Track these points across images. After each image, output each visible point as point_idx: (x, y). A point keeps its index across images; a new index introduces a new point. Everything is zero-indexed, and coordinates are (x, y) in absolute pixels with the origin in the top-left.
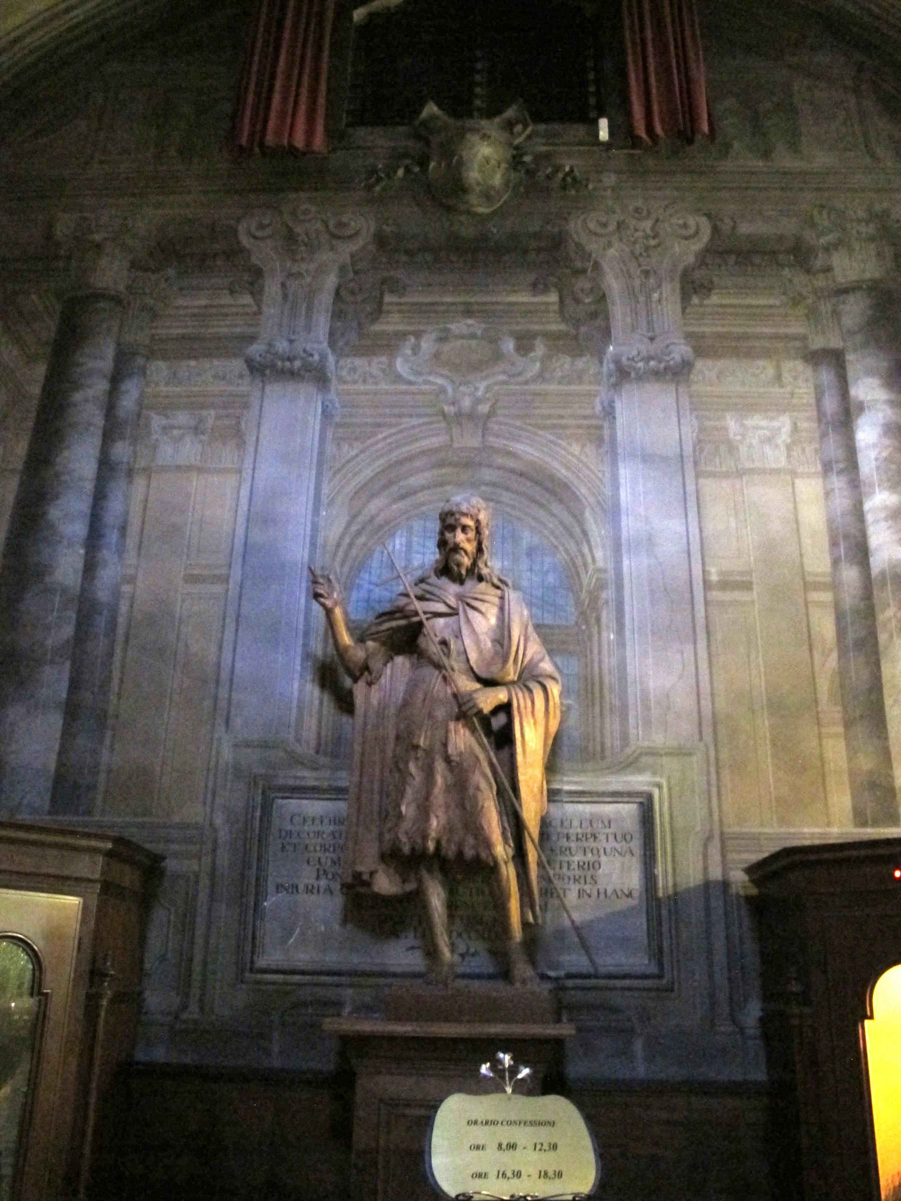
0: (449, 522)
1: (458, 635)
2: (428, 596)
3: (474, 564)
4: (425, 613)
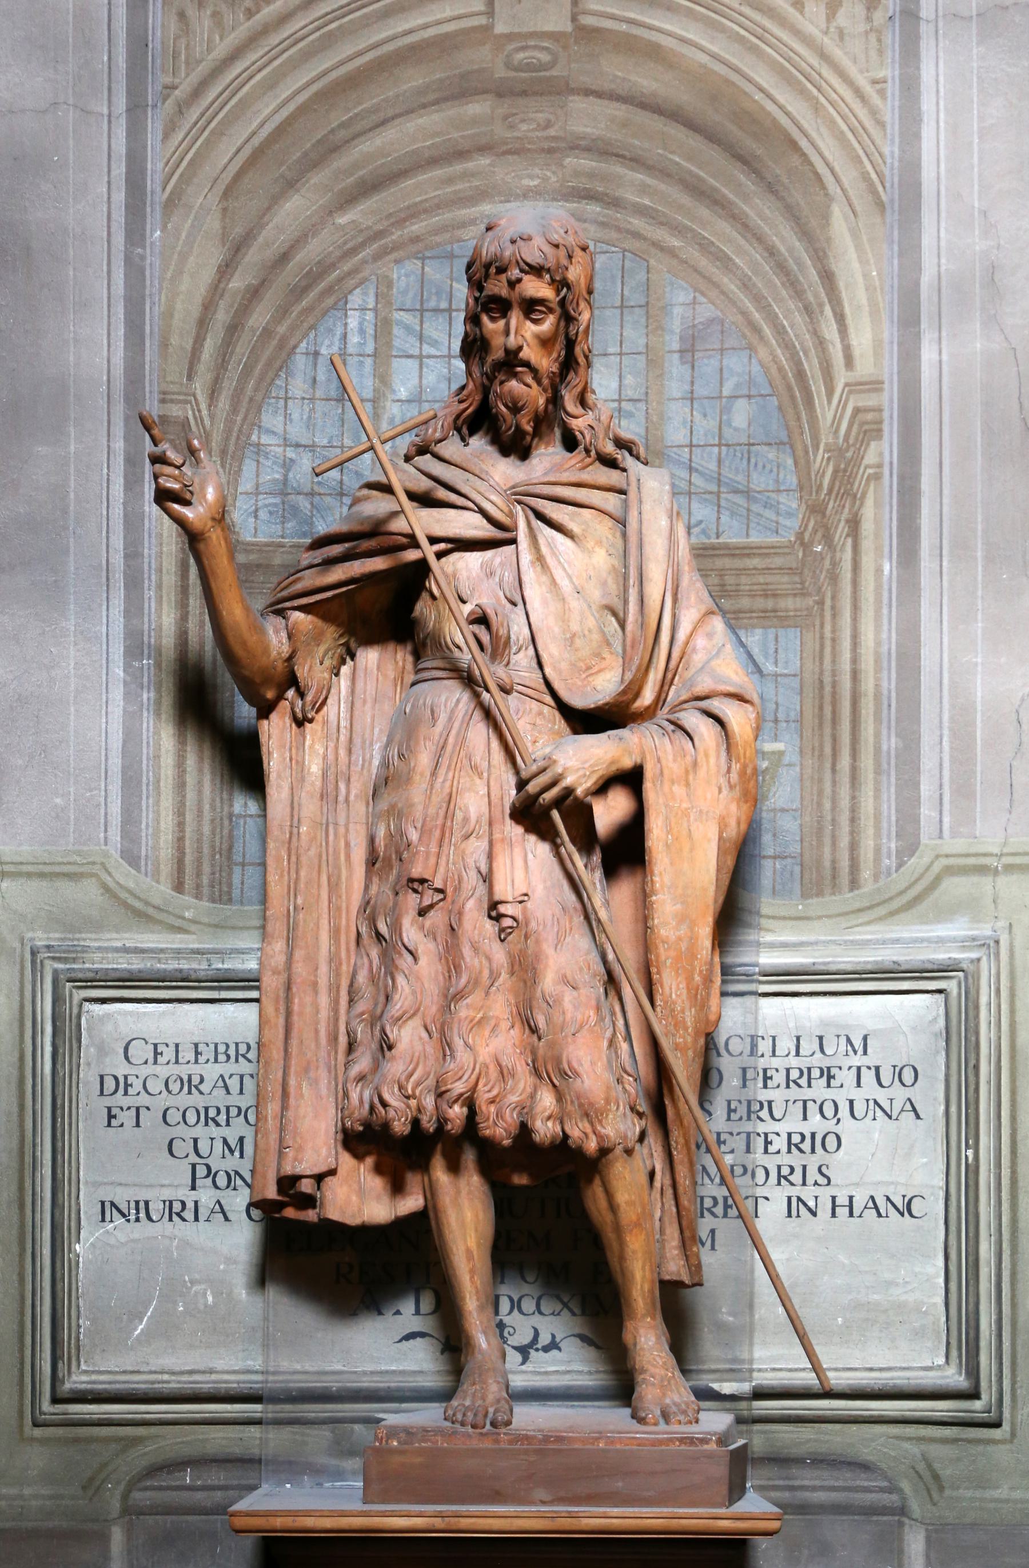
0: (490, 290)
1: (518, 600)
2: (442, 494)
3: (555, 400)
4: (433, 540)
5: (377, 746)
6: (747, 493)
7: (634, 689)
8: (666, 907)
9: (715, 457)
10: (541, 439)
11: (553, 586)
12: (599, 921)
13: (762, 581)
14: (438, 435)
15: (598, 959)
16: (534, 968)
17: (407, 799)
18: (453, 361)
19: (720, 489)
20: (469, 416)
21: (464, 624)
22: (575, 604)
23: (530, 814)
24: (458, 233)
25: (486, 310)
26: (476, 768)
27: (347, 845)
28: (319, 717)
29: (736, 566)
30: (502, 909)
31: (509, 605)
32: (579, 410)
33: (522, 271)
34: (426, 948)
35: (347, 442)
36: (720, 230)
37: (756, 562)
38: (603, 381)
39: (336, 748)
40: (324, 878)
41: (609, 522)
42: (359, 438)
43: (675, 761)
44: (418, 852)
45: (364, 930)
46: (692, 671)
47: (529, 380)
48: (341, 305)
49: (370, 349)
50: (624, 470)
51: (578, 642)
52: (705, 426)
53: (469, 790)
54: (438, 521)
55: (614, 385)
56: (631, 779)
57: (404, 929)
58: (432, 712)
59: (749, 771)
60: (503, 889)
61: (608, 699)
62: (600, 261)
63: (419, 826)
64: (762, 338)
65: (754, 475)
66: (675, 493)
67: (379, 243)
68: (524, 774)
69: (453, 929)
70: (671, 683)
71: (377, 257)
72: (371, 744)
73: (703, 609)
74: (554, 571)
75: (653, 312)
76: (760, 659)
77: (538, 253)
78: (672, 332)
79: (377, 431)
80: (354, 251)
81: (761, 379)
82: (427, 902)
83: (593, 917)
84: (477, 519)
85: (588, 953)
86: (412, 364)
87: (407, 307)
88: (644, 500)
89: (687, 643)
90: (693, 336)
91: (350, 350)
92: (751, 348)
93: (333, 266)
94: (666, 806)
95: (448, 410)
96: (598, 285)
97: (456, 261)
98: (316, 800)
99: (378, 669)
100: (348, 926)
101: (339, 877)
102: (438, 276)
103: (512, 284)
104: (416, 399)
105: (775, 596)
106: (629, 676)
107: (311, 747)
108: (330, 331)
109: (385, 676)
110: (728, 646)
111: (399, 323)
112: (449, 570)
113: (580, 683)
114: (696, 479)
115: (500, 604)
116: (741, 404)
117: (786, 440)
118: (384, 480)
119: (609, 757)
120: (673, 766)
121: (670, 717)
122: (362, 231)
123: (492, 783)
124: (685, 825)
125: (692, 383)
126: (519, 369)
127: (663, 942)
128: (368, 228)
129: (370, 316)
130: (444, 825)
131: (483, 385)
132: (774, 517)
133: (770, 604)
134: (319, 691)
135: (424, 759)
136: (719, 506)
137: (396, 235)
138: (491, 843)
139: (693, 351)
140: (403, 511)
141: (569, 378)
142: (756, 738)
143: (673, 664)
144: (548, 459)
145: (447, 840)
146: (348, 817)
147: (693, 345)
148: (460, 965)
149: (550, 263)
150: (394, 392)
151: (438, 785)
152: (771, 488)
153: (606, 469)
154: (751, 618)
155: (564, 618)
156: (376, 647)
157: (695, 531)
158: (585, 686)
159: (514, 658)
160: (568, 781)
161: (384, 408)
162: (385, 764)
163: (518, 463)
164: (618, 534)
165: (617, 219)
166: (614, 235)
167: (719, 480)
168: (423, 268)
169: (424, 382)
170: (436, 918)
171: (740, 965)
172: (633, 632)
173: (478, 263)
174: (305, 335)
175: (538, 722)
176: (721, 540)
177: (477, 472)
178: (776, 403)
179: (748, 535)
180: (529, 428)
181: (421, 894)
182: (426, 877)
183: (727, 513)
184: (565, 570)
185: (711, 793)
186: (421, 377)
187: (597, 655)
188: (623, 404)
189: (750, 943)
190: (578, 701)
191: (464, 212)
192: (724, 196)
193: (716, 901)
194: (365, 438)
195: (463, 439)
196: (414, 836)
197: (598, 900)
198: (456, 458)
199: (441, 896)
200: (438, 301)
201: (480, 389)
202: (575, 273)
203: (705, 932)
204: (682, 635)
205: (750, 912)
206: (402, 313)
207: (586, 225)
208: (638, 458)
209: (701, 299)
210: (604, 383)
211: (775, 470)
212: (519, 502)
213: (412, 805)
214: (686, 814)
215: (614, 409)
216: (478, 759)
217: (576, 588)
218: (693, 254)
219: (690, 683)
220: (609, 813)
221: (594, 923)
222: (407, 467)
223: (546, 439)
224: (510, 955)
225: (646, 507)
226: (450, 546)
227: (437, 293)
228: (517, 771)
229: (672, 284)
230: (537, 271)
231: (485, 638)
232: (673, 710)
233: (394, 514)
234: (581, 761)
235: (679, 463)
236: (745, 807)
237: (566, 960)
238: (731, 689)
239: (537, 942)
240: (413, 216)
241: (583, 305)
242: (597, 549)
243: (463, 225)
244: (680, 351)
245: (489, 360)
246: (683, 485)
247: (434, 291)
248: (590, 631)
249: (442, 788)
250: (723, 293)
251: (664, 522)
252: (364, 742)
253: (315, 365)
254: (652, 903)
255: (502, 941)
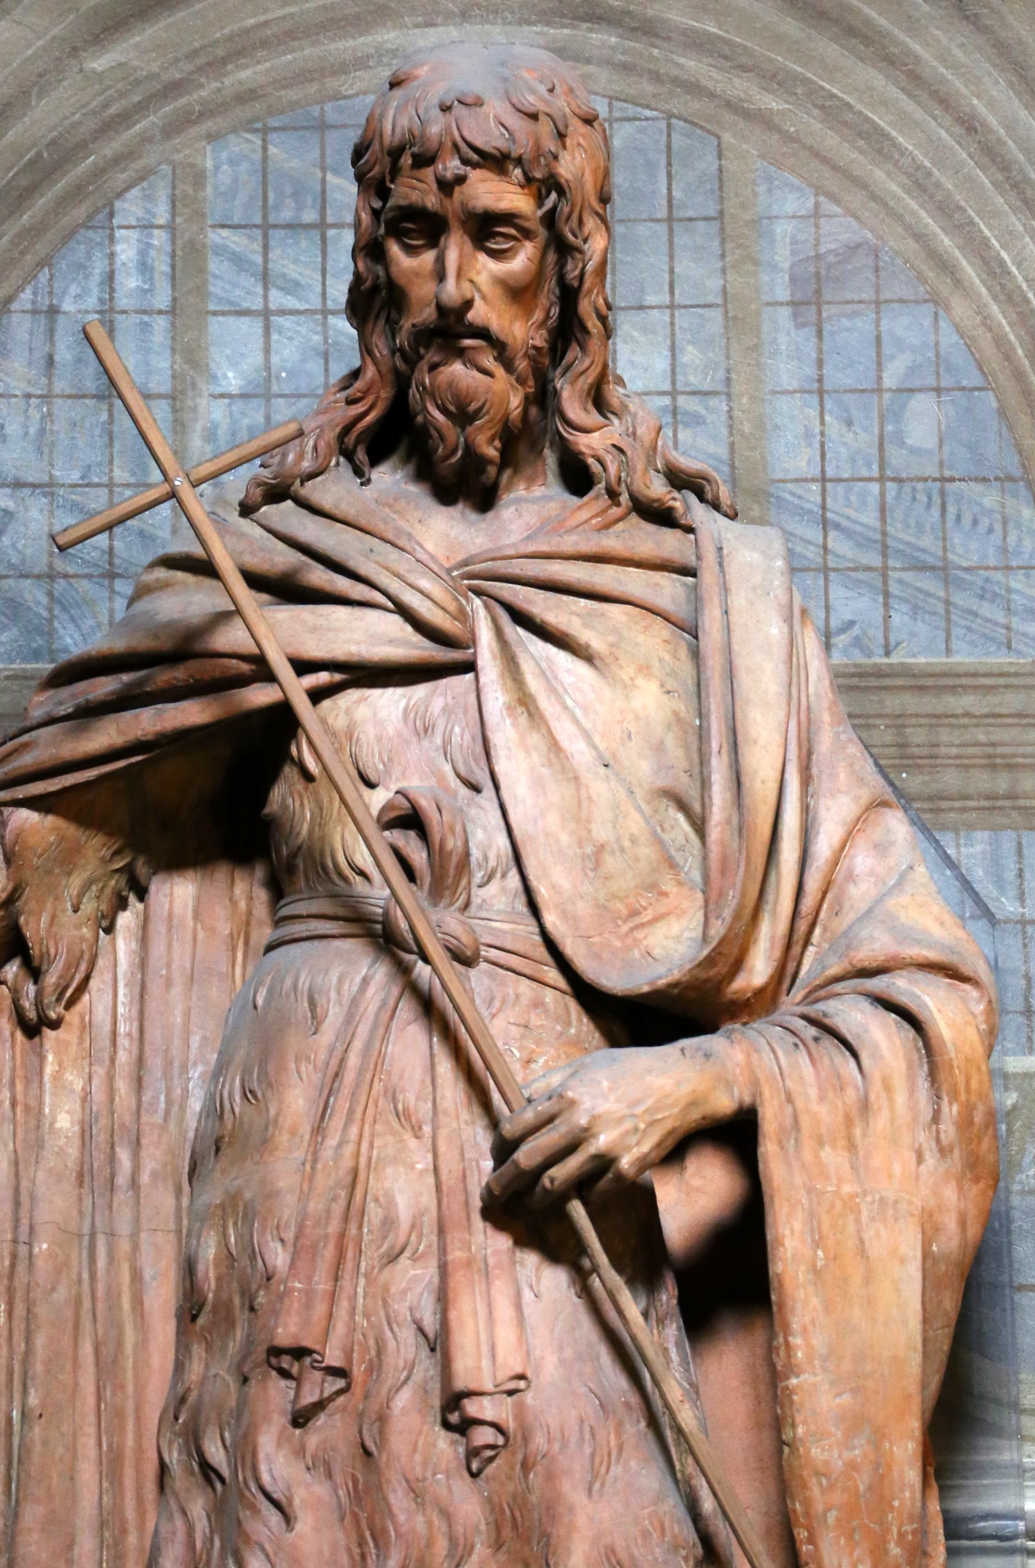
0: (403, 194)
1: (483, 779)
2: (319, 577)
3: (543, 397)
4: (303, 667)
5: (196, 1073)
6: (943, 570)
7: (730, 954)
8: (819, 1399)
9: (873, 503)
10: (516, 471)
11: (556, 754)
12: (679, 1431)
13: (982, 737)
14: (307, 465)
15: (681, 1512)
16: (546, 1537)
17: (263, 1182)
18: (332, 320)
19: (886, 564)
20: (368, 428)
21: (371, 829)
22: (600, 788)
23: (525, 1209)
24: (332, 83)
25: (396, 231)
26: (408, 1118)
27: (137, 1276)
28: (72, 1017)
29: (929, 709)
30: (472, 1408)
31: (464, 791)
32: (593, 418)
33: (465, 162)
34: (311, 1496)
35: (120, 475)
36: (862, 84)
37: (966, 702)
38: (638, 359)
39: (110, 1078)
40: (87, 1349)
41: (663, 630)
42: (145, 472)
43: (822, 1098)
44: (288, 1292)
45: (174, 1457)
46: (848, 917)
47: (488, 361)
48: (103, 220)
49: (162, 299)
50: (689, 530)
51: (610, 862)
52: (851, 444)
53: (395, 1161)
54: (314, 629)
55: (662, 364)
56: (735, 1135)
57: (261, 1456)
58: (312, 1004)
59: (978, 1118)
60: (471, 1367)
61: (676, 975)
62: (621, 136)
63: (290, 1235)
64: (958, 282)
65: (957, 539)
66: (794, 570)
67: (178, 105)
68: (509, 1129)
69: (367, 1453)
70: (807, 942)
71: (171, 130)
72: (184, 1068)
73: (865, 795)
74: (554, 725)
75: (734, 232)
76: (986, 889)
77: (496, 130)
78: (774, 267)
79: (179, 453)
80: (125, 119)
81: (960, 358)
82: (309, 1397)
83: (665, 1420)
84: (395, 624)
85: (659, 1499)
86: (251, 328)
87: (236, 221)
88: (733, 586)
89: (835, 862)
90: (817, 274)
91: (122, 301)
92: (935, 300)
93: (82, 148)
94: (810, 1191)
95: (324, 419)
96: (619, 179)
97: (331, 136)
98: (68, 1186)
99: (197, 915)
100: (139, 1449)
101: (120, 1344)
102: (295, 163)
103: (447, 186)
104: (261, 391)
105: (1010, 767)
106: (718, 929)
107: (57, 1077)
108: (80, 267)
109: (212, 930)
110: (921, 870)
111: (220, 250)
112: (339, 723)
113: (618, 944)
114: (836, 541)
115: (447, 789)
116: (922, 404)
117: (1018, 473)
118: (198, 551)
119: (685, 1091)
120: (820, 1111)
121: (811, 1010)
122: (137, 83)
123: (442, 1148)
124: (851, 1228)
125: (820, 363)
126: (468, 342)
127: (818, 1474)
128: (151, 77)
129: (160, 238)
130: (342, 1235)
131: (396, 372)
132: (1001, 617)
133: (1002, 783)
134: (73, 965)
135: (296, 1101)
136: (887, 594)
137: (207, 90)
138: (444, 1270)
139: (819, 305)
140: (238, 612)
141: (569, 356)
142: (990, 1050)
143: (808, 903)
144: (530, 512)
145: (349, 1265)
146: (137, 1220)
147: (818, 291)
148: (384, 1531)
149: (522, 147)
150: (214, 379)
151: (327, 1153)
152: (992, 562)
153: (651, 528)
154: (964, 810)
155: (578, 815)
156: (191, 874)
157: (840, 641)
158: (629, 949)
159: (479, 895)
160: (602, 1141)
161: (195, 410)
162: (215, 1110)
163: (473, 516)
164: (683, 653)
165: (652, 58)
166: (649, 88)
167: (885, 546)
168: (265, 149)
169: (275, 359)
170: (330, 1430)
171: (986, 1517)
172: (723, 844)
173: (376, 146)
174: (30, 277)
175: (535, 1020)
176: (894, 659)
177: (390, 536)
178: (995, 405)
179: (948, 651)
180: (492, 452)
181: (298, 1380)
182: (308, 1343)
183: (904, 607)
184: (577, 722)
185: (902, 1163)
186: (267, 351)
187: (652, 886)
188: (682, 401)
189: (1001, 1470)
190: (616, 979)
191: (341, 45)
192: (867, 21)
193: (924, 1385)
194: (156, 476)
195: (358, 472)
196: (279, 1257)
197: (674, 1390)
198: (346, 508)
199: (341, 1383)
200: (300, 207)
201: (390, 378)
202: (571, 165)
203: (906, 1451)
204: (823, 847)
205: (999, 1402)
206: (225, 233)
207: (591, 69)
208: (716, 506)
209: (829, 206)
210: (639, 359)
211: (998, 527)
212: (479, 593)
213: (271, 1195)
214: (851, 1206)
215: (664, 410)
216: (411, 1098)
217: (600, 756)
218: (810, 124)
219: (846, 941)
220: (690, 1201)
221: (669, 1434)
222: (246, 525)
223: (528, 471)
224: (492, 1505)
225: (738, 601)
226: (338, 677)
227: (296, 195)
228: (494, 1123)
229: (769, 179)
230: (496, 162)
231: (418, 856)
232: (813, 995)
233: (222, 617)
234: (625, 1100)
235: (800, 512)
236: (974, 1191)
237: (613, 1507)
238: (932, 955)
239: (550, 1476)
240: (239, 54)
241: (591, 223)
242: (640, 681)
243: (342, 69)
244: (792, 303)
245: (406, 324)
246: (813, 554)
247: (288, 190)
248: (633, 840)
249: (337, 1157)
250: (874, 197)
251: (776, 630)
252: (168, 1064)
253: (51, 331)
254: (789, 1392)
255: (474, 1475)
